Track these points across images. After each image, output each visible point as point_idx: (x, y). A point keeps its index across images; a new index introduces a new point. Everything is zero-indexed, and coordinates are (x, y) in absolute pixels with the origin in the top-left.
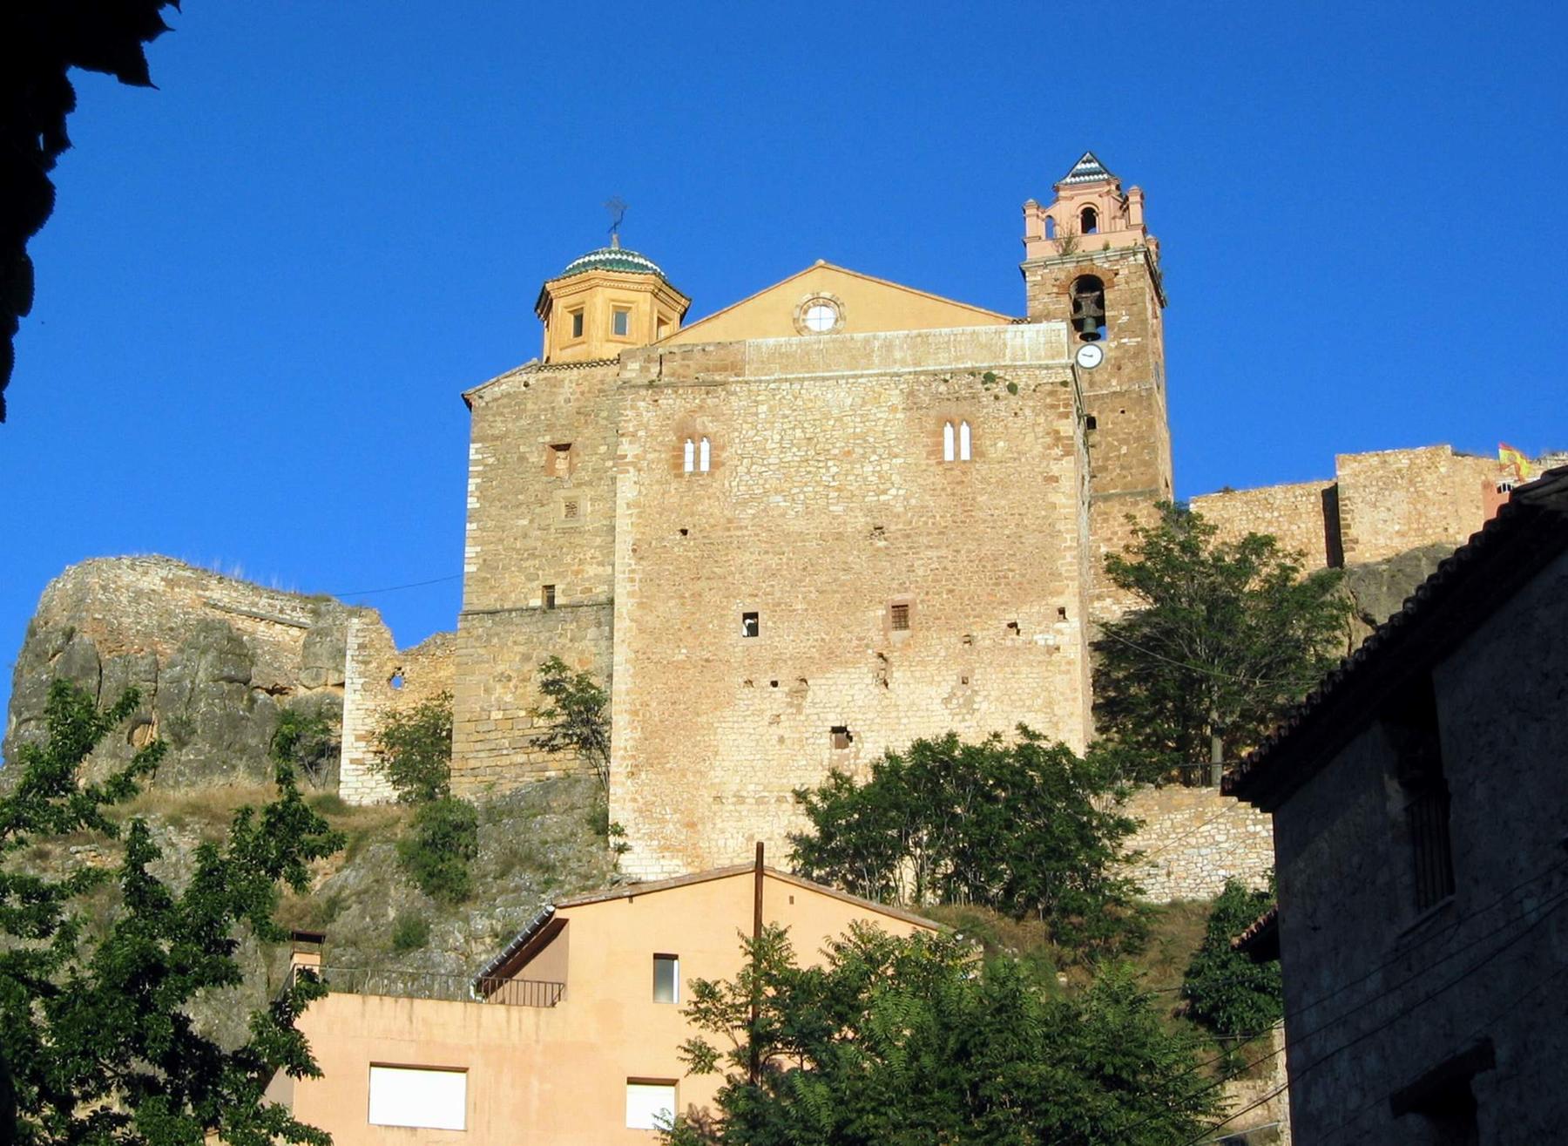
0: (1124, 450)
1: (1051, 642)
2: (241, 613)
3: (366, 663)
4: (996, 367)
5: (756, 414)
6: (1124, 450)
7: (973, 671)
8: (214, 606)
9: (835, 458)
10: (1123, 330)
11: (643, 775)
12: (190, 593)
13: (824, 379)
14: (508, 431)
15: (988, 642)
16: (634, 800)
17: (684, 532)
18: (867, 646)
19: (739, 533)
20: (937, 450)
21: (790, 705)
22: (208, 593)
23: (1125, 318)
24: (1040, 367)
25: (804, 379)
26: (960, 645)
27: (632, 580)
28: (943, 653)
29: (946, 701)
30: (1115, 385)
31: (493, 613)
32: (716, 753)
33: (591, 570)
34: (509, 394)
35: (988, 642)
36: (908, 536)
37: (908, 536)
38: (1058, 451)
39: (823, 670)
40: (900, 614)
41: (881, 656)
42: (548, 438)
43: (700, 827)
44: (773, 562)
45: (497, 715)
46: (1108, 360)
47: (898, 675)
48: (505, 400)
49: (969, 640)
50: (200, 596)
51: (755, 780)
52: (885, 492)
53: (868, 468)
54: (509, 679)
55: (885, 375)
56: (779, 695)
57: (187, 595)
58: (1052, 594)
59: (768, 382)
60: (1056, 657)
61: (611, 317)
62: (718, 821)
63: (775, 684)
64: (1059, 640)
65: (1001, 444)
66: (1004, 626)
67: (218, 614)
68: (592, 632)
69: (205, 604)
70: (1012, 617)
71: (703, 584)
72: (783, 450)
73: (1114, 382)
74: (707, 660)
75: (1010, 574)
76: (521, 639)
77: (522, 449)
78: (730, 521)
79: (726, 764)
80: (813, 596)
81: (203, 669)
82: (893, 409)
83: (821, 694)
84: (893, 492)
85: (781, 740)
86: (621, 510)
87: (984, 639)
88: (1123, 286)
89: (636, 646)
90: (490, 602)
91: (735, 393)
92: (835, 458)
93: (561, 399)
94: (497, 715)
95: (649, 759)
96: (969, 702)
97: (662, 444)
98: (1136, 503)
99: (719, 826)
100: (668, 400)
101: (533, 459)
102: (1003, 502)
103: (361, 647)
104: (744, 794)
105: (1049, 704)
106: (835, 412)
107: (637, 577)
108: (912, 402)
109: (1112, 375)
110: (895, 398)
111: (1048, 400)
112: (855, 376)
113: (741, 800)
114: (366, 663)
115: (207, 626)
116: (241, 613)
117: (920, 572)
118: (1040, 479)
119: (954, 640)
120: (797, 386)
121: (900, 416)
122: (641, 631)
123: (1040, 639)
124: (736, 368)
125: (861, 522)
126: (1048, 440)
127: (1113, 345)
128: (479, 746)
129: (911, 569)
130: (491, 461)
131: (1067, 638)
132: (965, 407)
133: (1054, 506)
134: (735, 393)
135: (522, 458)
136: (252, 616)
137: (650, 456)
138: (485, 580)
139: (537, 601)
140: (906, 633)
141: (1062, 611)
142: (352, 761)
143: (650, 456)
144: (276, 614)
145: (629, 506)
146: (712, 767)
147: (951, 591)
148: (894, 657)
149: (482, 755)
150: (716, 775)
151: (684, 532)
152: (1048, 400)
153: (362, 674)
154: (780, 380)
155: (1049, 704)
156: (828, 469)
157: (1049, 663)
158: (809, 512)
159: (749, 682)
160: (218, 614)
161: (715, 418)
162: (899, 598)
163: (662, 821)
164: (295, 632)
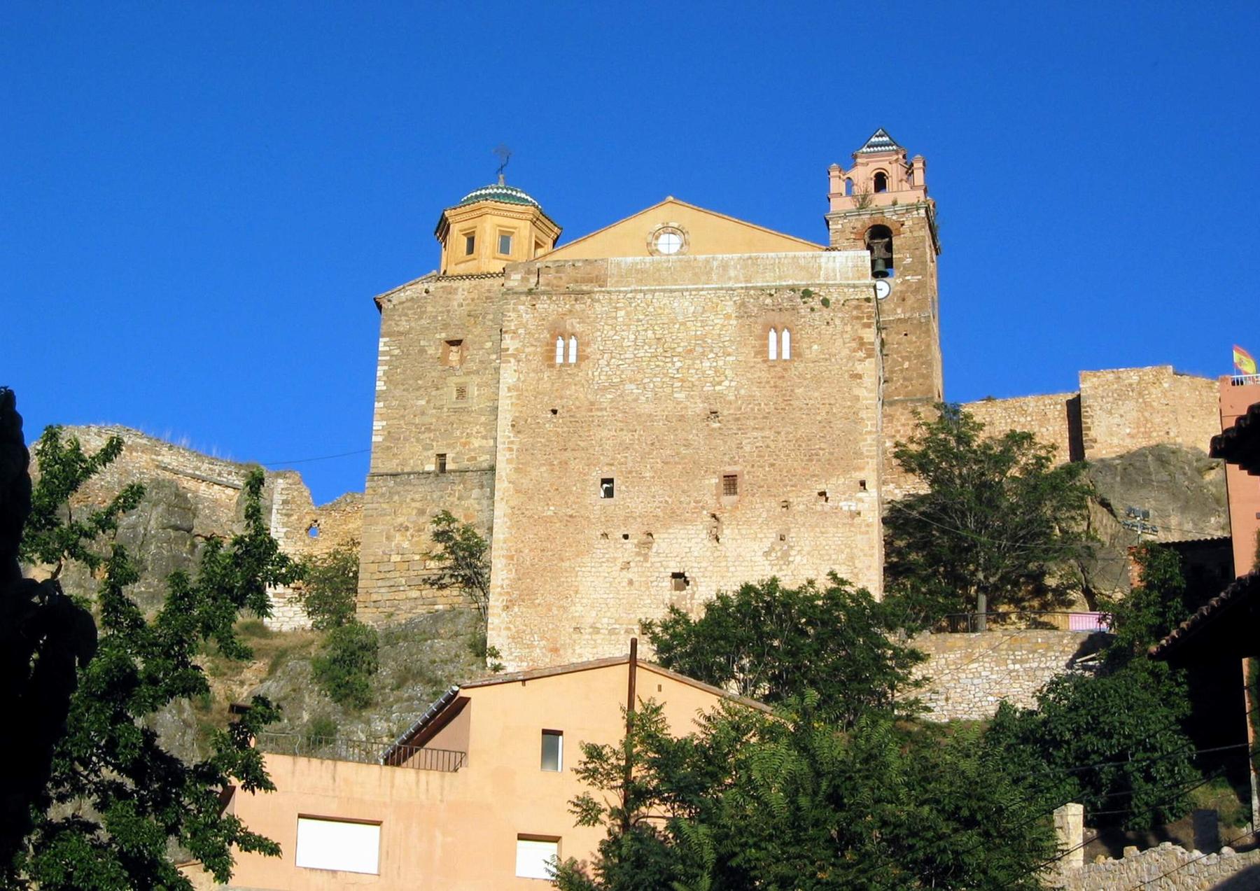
0: (906, 365)
1: (853, 508)
2: (186, 475)
3: (288, 515)
4: (812, 285)
5: (616, 318)
7: (789, 530)
8: (165, 469)
9: (679, 355)
10: (907, 270)
11: (516, 609)
12: (145, 457)
13: (671, 291)
14: (411, 328)
16: (509, 629)
17: (555, 412)
18: (703, 508)
19: (599, 414)
20: (763, 351)
21: (638, 554)
22: (160, 458)
23: (909, 260)
24: (848, 286)
25: (655, 291)
26: (779, 509)
27: (511, 450)
28: (764, 515)
29: (767, 554)
32: (577, 592)
34: (412, 299)
35: (801, 507)
36: (738, 419)
37: (738, 419)
38: (861, 354)
39: (666, 526)
40: (731, 483)
41: (714, 516)
42: (443, 335)
43: (562, 652)
44: (627, 437)
45: (396, 558)
46: (894, 293)
47: (727, 533)
48: (409, 304)
50: (153, 460)
51: (609, 614)
52: (720, 383)
54: (407, 529)
55: (722, 289)
56: (629, 546)
58: (855, 469)
59: (626, 292)
60: (857, 520)
61: (498, 240)
62: (577, 647)
63: (626, 537)
64: (860, 507)
65: (815, 347)
66: (816, 494)
67: (168, 475)
68: (476, 492)
69: (157, 467)
70: (822, 487)
71: (568, 454)
72: (637, 347)
73: (899, 311)
74: (571, 516)
75: (821, 452)
76: (417, 497)
77: (422, 343)
78: (592, 404)
79: (585, 601)
80: (659, 466)
82: (728, 317)
83: (664, 545)
84: (726, 383)
85: (631, 582)
86: (503, 392)
87: (799, 505)
88: (908, 234)
89: (512, 503)
90: (392, 466)
91: (599, 301)
92: (679, 355)
93: (455, 303)
94: (396, 558)
95: (520, 596)
96: (786, 555)
97: (537, 340)
99: (578, 651)
100: (543, 305)
101: (431, 351)
102: (816, 394)
103: (285, 502)
104: (599, 625)
106: (680, 318)
107: (515, 447)
108: (743, 311)
109: (897, 306)
110: (730, 308)
111: (855, 313)
112: (696, 290)
113: (596, 630)
114: (288, 515)
116: (186, 475)
117: (747, 449)
118: (846, 376)
119: (774, 504)
120: (649, 296)
121: (734, 322)
122: (518, 491)
123: (845, 506)
124: (600, 280)
125: (700, 407)
126: (854, 345)
127: (899, 281)
128: (380, 583)
129: (740, 446)
130: (396, 352)
131: (866, 505)
132: (786, 317)
133: (857, 398)
134: (599, 301)
135: (422, 351)
136: (194, 477)
138: (389, 448)
139: (431, 467)
140: (735, 498)
141: (863, 484)
143: (527, 350)
144: (215, 476)
145: (509, 390)
147: (772, 465)
148: (724, 517)
149: (383, 590)
150: (577, 610)
151: (555, 412)
152: (855, 313)
153: (284, 525)
154: (636, 291)
155: (852, 558)
156: (673, 363)
157: (852, 525)
158: (657, 398)
159: (605, 535)
160: (168, 475)
161: (582, 321)
162: (730, 470)
163: (531, 646)
164: (230, 491)
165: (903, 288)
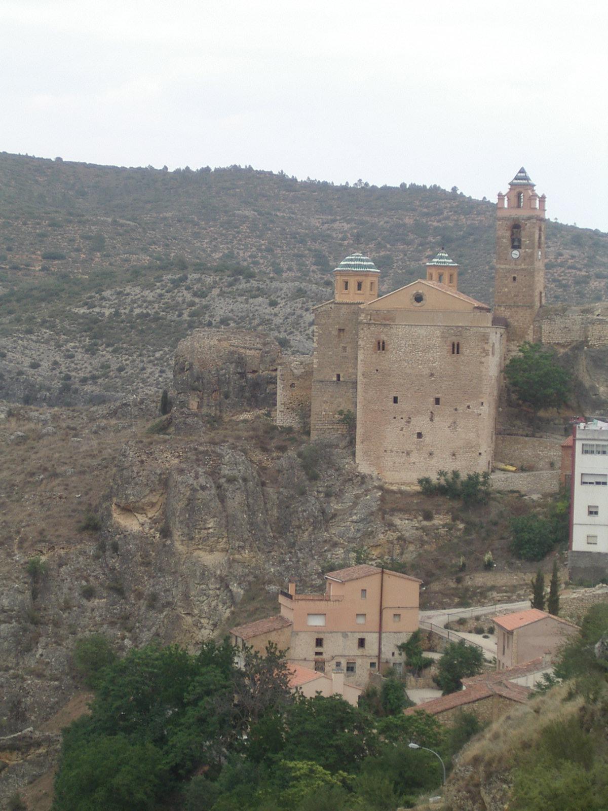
0: (524, 290)
3: (284, 381)
6: (524, 290)
10: (527, 247)
12: (226, 343)
14: (326, 323)
15: (461, 411)
17: (377, 370)
21: (406, 425)
23: (528, 242)
29: (449, 427)
30: (523, 266)
31: (322, 381)
33: (350, 370)
34: (325, 311)
35: (461, 411)
40: (437, 401)
41: (431, 412)
45: (324, 413)
47: (436, 419)
48: (324, 313)
49: (456, 410)
52: (435, 363)
53: (430, 355)
54: (327, 403)
57: (225, 344)
60: (480, 417)
61: (357, 284)
63: (402, 418)
64: (481, 412)
67: (235, 349)
68: (351, 391)
70: (468, 404)
76: (331, 390)
77: (330, 329)
78: (390, 368)
81: (232, 368)
85: (404, 435)
86: (359, 362)
89: (363, 404)
90: (321, 378)
92: (421, 351)
94: (324, 413)
97: (371, 342)
98: (527, 310)
99: (386, 459)
100: (372, 328)
101: (333, 332)
103: (282, 375)
105: (477, 430)
109: (522, 262)
113: (392, 451)
114: (284, 381)
115: (232, 353)
117: (444, 388)
122: (365, 399)
124: (393, 320)
125: (426, 372)
126: (482, 350)
127: (523, 251)
128: (319, 422)
129: (441, 387)
130: (321, 332)
133: (482, 372)
135: (330, 333)
136: (245, 348)
137: (368, 346)
138: (319, 370)
139: (335, 379)
141: (482, 403)
142: (280, 411)
143: (368, 346)
144: (252, 346)
145: (361, 361)
146: (384, 442)
151: (377, 370)
153: (282, 384)
155: (477, 430)
159: (395, 418)
164: (258, 351)
165: (525, 254)
